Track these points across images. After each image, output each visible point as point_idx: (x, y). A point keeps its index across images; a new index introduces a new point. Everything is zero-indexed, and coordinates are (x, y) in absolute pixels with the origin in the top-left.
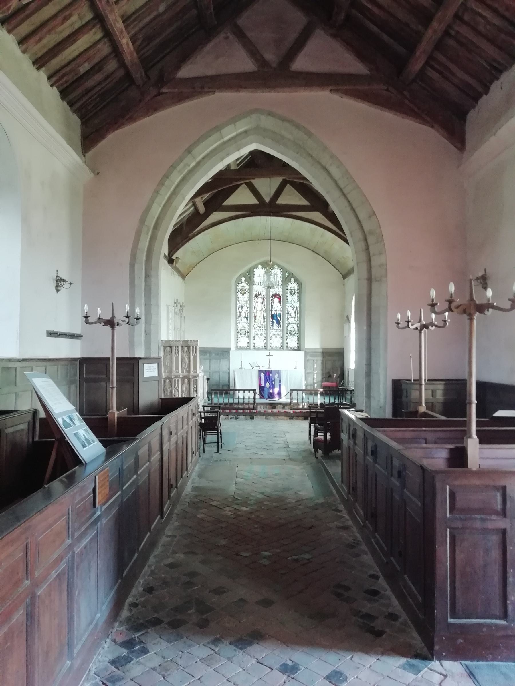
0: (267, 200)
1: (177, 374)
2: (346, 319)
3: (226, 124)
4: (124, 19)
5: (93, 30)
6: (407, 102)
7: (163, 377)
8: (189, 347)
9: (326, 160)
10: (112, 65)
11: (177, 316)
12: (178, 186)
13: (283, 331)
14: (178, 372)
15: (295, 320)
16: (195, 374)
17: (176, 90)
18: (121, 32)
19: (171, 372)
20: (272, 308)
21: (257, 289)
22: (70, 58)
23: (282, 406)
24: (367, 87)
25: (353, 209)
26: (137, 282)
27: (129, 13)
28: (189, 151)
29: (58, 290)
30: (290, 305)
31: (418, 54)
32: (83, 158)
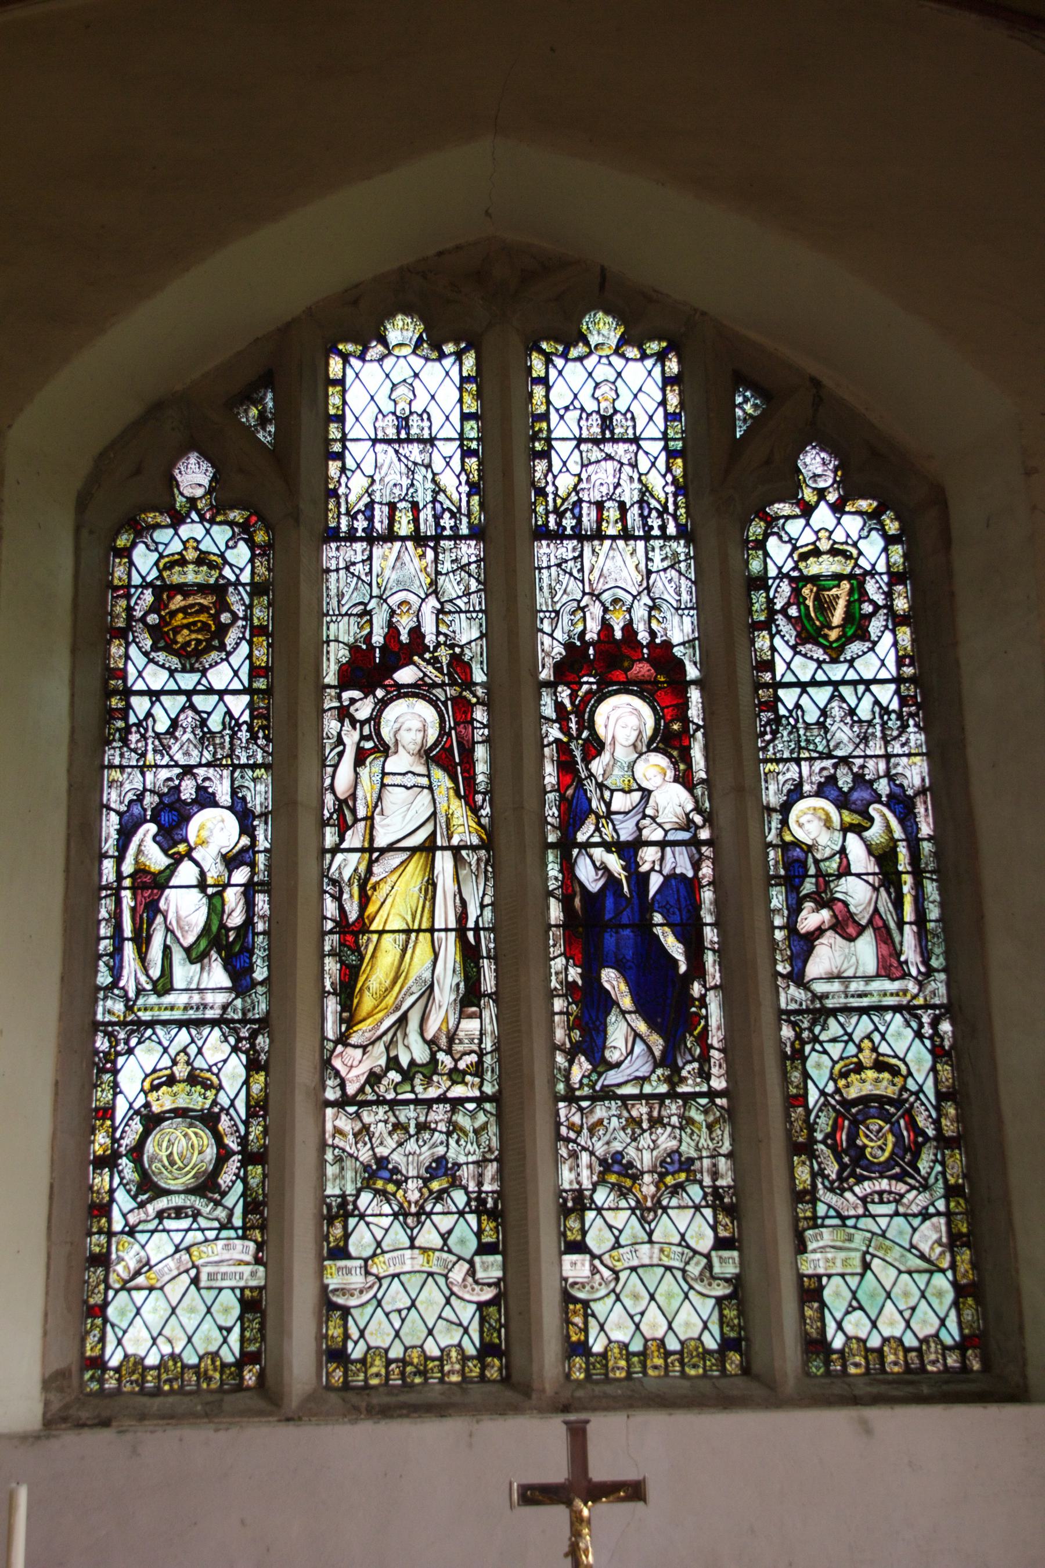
13: (735, 1110)
15: (890, 965)
20: (574, 812)
30: (812, 773)
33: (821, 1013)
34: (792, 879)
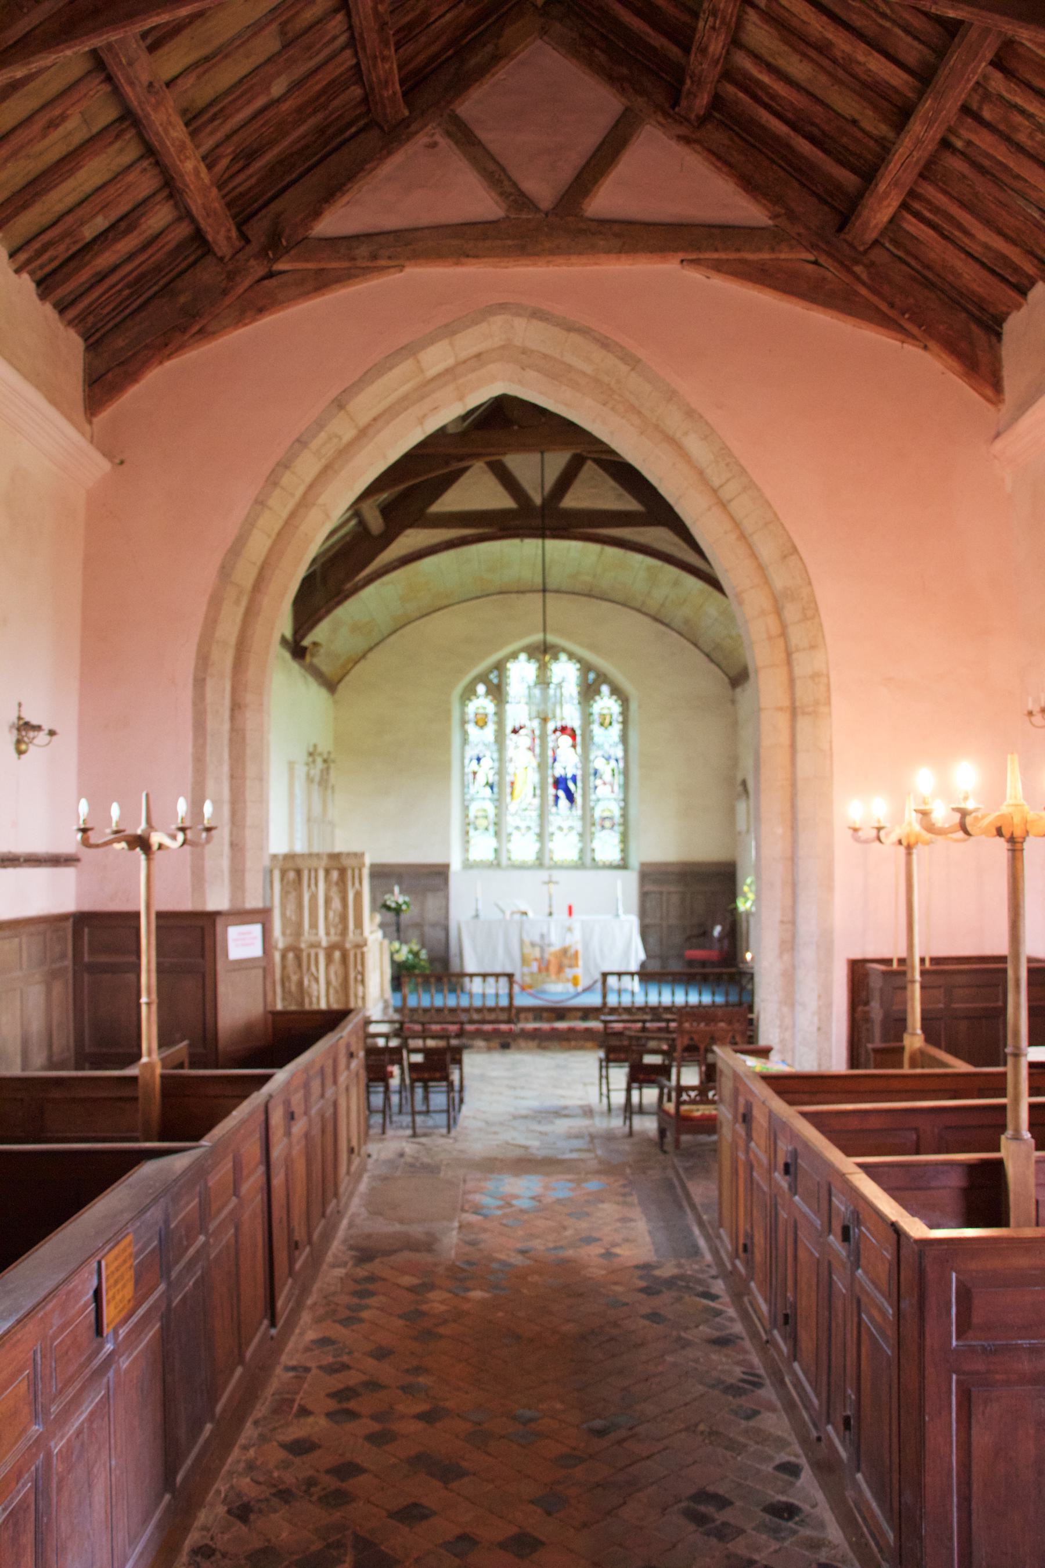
0: (538, 500)
1: (313, 939)
2: (740, 789)
3: (431, 340)
4: (190, 116)
5: (117, 145)
6: (863, 291)
7: (281, 945)
8: (342, 871)
9: (674, 421)
10: (160, 217)
11: (315, 787)
12: (311, 487)
13: (583, 818)
14: (317, 934)
15: (613, 792)
16: (359, 939)
17: (310, 266)
18: (183, 147)
19: (298, 933)
20: (555, 760)
21: (517, 712)
22: (60, 208)
23: (579, 1014)
24: (766, 256)
25: (743, 537)
26: (210, 724)
27: (200, 103)
28: (340, 404)
29: (20, 753)
30: (600, 753)
31: (882, 187)
32: (87, 427)
33: (598, 800)
34: (595, 773)
